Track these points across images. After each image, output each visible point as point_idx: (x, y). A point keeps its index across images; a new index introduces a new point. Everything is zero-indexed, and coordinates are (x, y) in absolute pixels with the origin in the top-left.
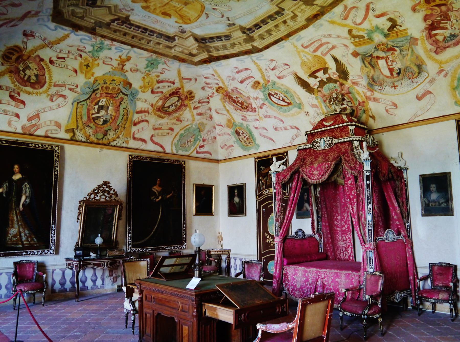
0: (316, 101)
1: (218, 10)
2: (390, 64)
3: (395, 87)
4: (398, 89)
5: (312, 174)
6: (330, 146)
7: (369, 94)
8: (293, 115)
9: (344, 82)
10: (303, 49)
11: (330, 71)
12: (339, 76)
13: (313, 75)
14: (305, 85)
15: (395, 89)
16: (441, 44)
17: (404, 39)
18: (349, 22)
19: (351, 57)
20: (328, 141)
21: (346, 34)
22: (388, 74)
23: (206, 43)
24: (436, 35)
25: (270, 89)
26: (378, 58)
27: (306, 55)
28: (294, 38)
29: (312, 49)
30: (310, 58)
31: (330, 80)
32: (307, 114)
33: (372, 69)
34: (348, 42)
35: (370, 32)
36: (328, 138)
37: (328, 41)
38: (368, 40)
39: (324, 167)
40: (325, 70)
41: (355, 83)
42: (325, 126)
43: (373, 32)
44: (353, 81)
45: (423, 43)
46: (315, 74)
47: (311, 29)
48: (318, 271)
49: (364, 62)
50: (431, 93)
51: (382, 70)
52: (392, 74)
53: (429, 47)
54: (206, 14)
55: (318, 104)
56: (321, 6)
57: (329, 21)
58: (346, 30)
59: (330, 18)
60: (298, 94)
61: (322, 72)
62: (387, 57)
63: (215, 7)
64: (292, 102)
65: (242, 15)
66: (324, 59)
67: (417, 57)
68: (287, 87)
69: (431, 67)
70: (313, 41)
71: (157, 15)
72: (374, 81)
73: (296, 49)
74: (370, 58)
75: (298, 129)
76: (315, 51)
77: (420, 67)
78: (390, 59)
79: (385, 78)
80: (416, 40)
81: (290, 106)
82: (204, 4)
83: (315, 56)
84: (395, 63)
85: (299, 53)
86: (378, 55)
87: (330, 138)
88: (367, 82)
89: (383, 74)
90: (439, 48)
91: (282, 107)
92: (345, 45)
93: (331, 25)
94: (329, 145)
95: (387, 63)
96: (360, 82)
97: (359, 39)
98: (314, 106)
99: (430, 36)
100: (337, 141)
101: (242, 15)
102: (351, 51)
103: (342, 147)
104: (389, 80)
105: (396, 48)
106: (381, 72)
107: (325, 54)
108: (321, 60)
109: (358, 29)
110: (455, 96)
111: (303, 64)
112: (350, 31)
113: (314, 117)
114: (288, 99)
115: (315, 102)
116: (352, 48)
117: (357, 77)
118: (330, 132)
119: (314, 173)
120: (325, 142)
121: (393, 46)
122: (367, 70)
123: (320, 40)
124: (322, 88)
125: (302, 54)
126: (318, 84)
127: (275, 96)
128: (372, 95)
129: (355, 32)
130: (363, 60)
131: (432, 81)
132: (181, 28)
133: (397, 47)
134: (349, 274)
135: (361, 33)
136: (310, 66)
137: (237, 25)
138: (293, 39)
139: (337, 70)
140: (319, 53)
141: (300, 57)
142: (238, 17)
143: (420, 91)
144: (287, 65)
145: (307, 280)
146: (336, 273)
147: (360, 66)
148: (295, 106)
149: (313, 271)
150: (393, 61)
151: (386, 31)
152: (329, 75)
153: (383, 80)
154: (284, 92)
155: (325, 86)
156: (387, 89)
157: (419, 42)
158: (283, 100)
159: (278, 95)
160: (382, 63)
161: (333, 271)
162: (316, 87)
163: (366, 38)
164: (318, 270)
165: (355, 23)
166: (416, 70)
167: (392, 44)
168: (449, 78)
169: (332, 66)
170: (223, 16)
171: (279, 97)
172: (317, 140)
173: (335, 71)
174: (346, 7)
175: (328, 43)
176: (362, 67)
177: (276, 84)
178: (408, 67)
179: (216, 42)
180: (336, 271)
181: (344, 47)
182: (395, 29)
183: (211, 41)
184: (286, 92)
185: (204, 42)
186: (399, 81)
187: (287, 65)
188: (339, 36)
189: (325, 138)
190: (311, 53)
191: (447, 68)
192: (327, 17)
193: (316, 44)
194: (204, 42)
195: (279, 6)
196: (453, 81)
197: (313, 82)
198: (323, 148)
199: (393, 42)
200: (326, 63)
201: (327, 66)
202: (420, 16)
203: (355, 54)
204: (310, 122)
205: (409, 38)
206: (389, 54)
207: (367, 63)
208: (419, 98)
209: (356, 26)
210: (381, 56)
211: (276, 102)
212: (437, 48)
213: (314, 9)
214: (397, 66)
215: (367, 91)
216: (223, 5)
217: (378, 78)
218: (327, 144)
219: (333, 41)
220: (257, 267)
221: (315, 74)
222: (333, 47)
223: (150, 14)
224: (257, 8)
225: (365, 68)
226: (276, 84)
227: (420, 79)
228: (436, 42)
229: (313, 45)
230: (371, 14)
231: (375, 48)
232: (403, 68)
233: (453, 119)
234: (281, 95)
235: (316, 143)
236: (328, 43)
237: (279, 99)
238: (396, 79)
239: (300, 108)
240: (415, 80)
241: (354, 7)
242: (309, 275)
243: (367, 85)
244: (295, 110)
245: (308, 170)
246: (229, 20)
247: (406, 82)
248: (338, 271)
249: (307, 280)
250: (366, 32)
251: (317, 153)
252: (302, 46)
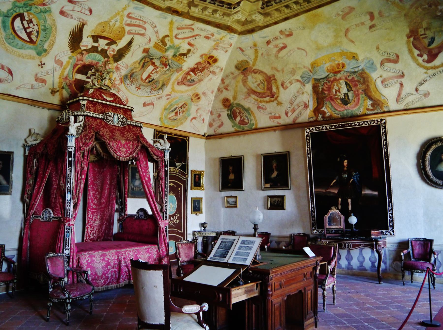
0: (68, 60)
2: (153, 72)
3: (139, 88)
4: (140, 91)
5: (119, 150)
6: (123, 125)
7: (118, 82)
8: (20, 55)
9: (112, 62)
10: (126, 15)
11: (113, 46)
12: (114, 56)
13: (96, 38)
14: (76, 38)
15: (138, 90)
16: (185, 81)
17: (178, 65)
18: (176, 32)
19: (142, 49)
20: (122, 119)
21: (161, 36)
22: (144, 78)
24: (190, 74)
25: (32, 12)
26: (153, 64)
27: (119, 20)
28: (138, 5)
29: (129, 21)
30: (116, 26)
31: (104, 53)
32: (42, 65)
33: (140, 67)
34: (154, 40)
35: (173, 47)
36: (122, 116)
37: (147, 29)
38: (164, 50)
39: (131, 146)
40: (112, 42)
41: (117, 68)
42: (104, 99)
43: (173, 48)
44: (119, 66)
45: (181, 74)
46: (99, 39)
47: (158, 13)
48: (119, 252)
49: (142, 59)
50: (153, 105)
51: (144, 73)
52: (146, 79)
53: (180, 79)
55: (65, 63)
56: (188, 12)
57: (172, 21)
58: (167, 33)
59: (176, 20)
60: (57, 40)
61: (107, 42)
62: (158, 68)
64: (39, 42)
66: (124, 35)
67: (169, 79)
68: (55, 25)
69: (167, 90)
70: (141, 19)
72: (131, 76)
73: (120, 10)
74: (149, 60)
75: (10, 73)
76: (129, 25)
77: (163, 85)
78: (157, 70)
79: (140, 79)
80: (181, 69)
81: (30, 45)
83: (123, 28)
84: (156, 74)
85: (118, 14)
86: (155, 62)
87: (123, 117)
88: (126, 74)
89: (142, 75)
90: (181, 83)
91: (17, 38)
92: (150, 40)
93: (168, 23)
94: (123, 123)
95: (153, 70)
96: (122, 71)
97: (163, 45)
98: (59, 62)
99: (188, 73)
100: (129, 123)
102: (147, 47)
103: (134, 129)
104: (140, 82)
105: (168, 67)
106: (142, 74)
107: (129, 33)
108: (121, 33)
109: (171, 40)
110: (162, 114)
111: (105, 24)
112: (167, 36)
113: (48, 72)
114: (37, 37)
115: (65, 60)
116: (152, 45)
117: (125, 65)
118: (113, 108)
119: (121, 149)
120: (119, 119)
121: (169, 64)
122: (137, 65)
123: (145, 23)
124: (89, 53)
125: (118, 17)
126: (89, 47)
127: (25, 22)
128: (119, 85)
129: (167, 40)
130: (144, 58)
131: (159, 98)
133: (169, 66)
134: (149, 249)
135: (169, 44)
136: (107, 30)
138: (136, 4)
139: (119, 51)
140: (127, 28)
141: (112, 18)
143: (148, 100)
144: (91, 11)
145: (108, 264)
146: (138, 250)
147: (137, 60)
148: (35, 49)
149: (112, 253)
150: (157, 72)
151: (178, 54)
152: (108, 48)
153: (137, 79)
154: (43, 27)
155: (93, 54)
156: (133, 87)
157: (180, 73)
158: (29, 35)
159: (31, 25)
160: (151, 68)
161: (133, 248)
162: (83, 48)
163: (166, 48)
164: (118, 250)
165: (177, 35)
166: (160, 85)
167: (170, 62)
168: (168, 101)
169: (122, 44)
171: (29, 27)
172: (110, 114)
173: (116, 50)
174: (192, 25)
175: (145, 29)
176: (137, 61)
177: (48, 13)
178: (158, 81)
180: (137, 248)
181: (148, 41)
182: (183, 56)
184: (45, 30)
186: (145, 86)
187: (91, 11)
188: (157, 32)
189: (119, 115)
190: (124, 23)
191: (173, 95)
192: (176, 18)
193: (138, 22)
196: (168, 104)
197: (87, 42)
198: (116, 124)
199: (172, 62)
200: (121, 39)
201: (117, 42)
202: (199, 60)
203: (146, 51)
204: (36, 75)
205: (180, 66)
206: (161, 66)
207: (143, 61)
208: (145, 105)
209: (174, 38)
210: (156, 64)
211: (16, 28)
212: (182, 81)
213: (184, 8)
214: (155, 76)
215: (119, 79)
217: (136, 76)
218: (121, 121)
219: (150, 32)
220: (59, 261)
221: (99, 39)
222: (142, 35)
225: (137, 63)
226: (46, 15)
227: (155, 93)
228: (185, 78)
229: (135, 21)
230: (190, 40)
231: (160, 57)
232: (156, 80)
233: (152, 128)
234: (36, 28)
235: (109, 116)
236: (145, 29)
237: (25, 29)
238: (144, 84)
239: (39, 54)
240: (153, 92)
241: (193, 29)
242: (109, 259)
243: (124, 76)
244: (33, 53)
245: (115, 144)
247: (148, 89)
248: (139, 248)
249: (108, 264)
250: (171, 45)
251: (110, 128)
252: (129, 14)
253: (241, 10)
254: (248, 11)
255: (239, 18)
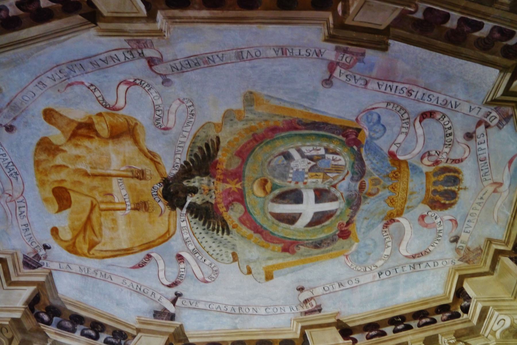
1: (182, 265)
23: (49, 323)
54: (149, 256)
63: (186, 255)
65: (214, 307)
71: (42, 184)
82: (178, 232)
101: (214, 307)
132: (42, 252)
137: (176, 323)
142: (201, 306)
170: (175, 284)
179: (78, 334)
183: (68, 325)
185: (46, 318)
194: (46, 318)
195: (307, 331)
216: (207, 262)
223: (32, 169)
224: (262, 311)
246: (174, 302)
253: (487, 304)
254: (508, 296)
255: (508, 324)
